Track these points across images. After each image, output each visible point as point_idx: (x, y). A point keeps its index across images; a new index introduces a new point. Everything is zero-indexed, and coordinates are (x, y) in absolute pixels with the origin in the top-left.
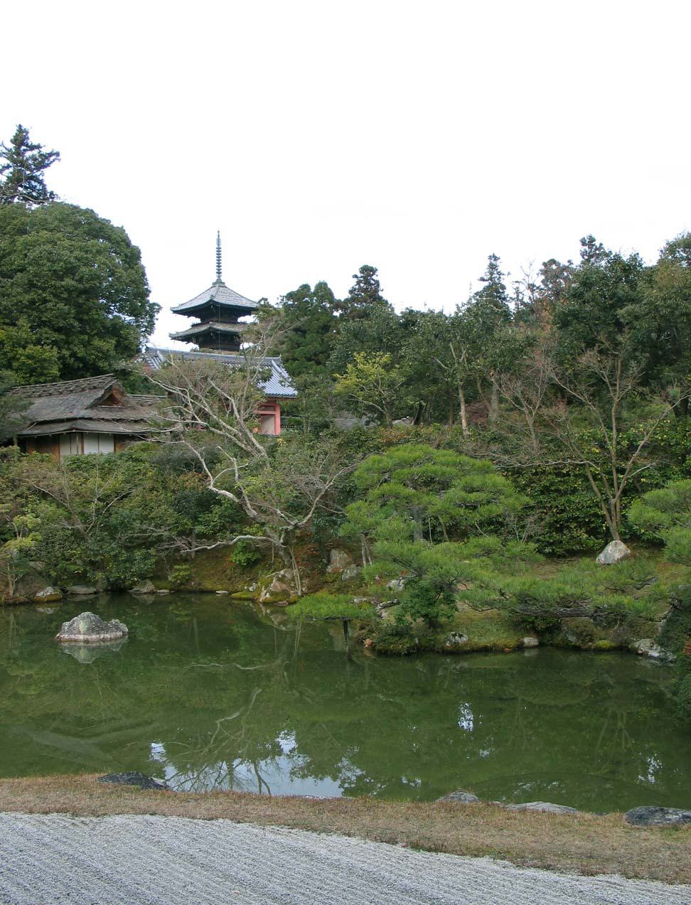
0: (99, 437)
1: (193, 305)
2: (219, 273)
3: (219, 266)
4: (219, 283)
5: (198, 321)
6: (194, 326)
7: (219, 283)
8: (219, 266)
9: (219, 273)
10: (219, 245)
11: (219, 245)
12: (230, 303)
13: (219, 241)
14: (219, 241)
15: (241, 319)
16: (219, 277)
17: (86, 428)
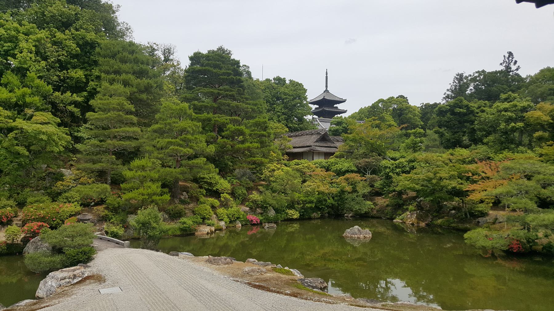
0: (319, 153)
1: (316, 100)
2: (327, 87)
3: (327, 84)
4: (326, 91)
5: (318, 106)
6: (316, 108)
7: (326, 91)
8: (327, 84)
9: (327, 87)
10: (327, 75)
11: (327, 75)
12: (331, 99)
13: (327, 73)
14: (327, 73)
15: (335, 106)
16: (327, 88)
17: (315, 149)
